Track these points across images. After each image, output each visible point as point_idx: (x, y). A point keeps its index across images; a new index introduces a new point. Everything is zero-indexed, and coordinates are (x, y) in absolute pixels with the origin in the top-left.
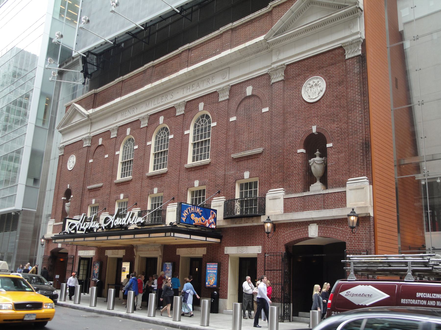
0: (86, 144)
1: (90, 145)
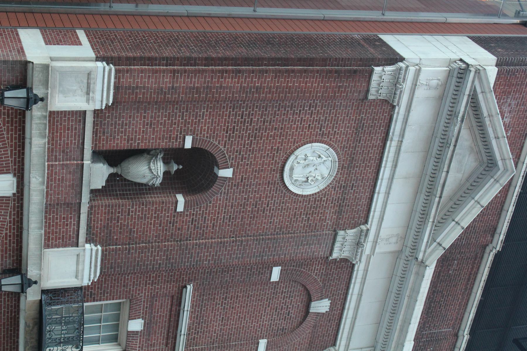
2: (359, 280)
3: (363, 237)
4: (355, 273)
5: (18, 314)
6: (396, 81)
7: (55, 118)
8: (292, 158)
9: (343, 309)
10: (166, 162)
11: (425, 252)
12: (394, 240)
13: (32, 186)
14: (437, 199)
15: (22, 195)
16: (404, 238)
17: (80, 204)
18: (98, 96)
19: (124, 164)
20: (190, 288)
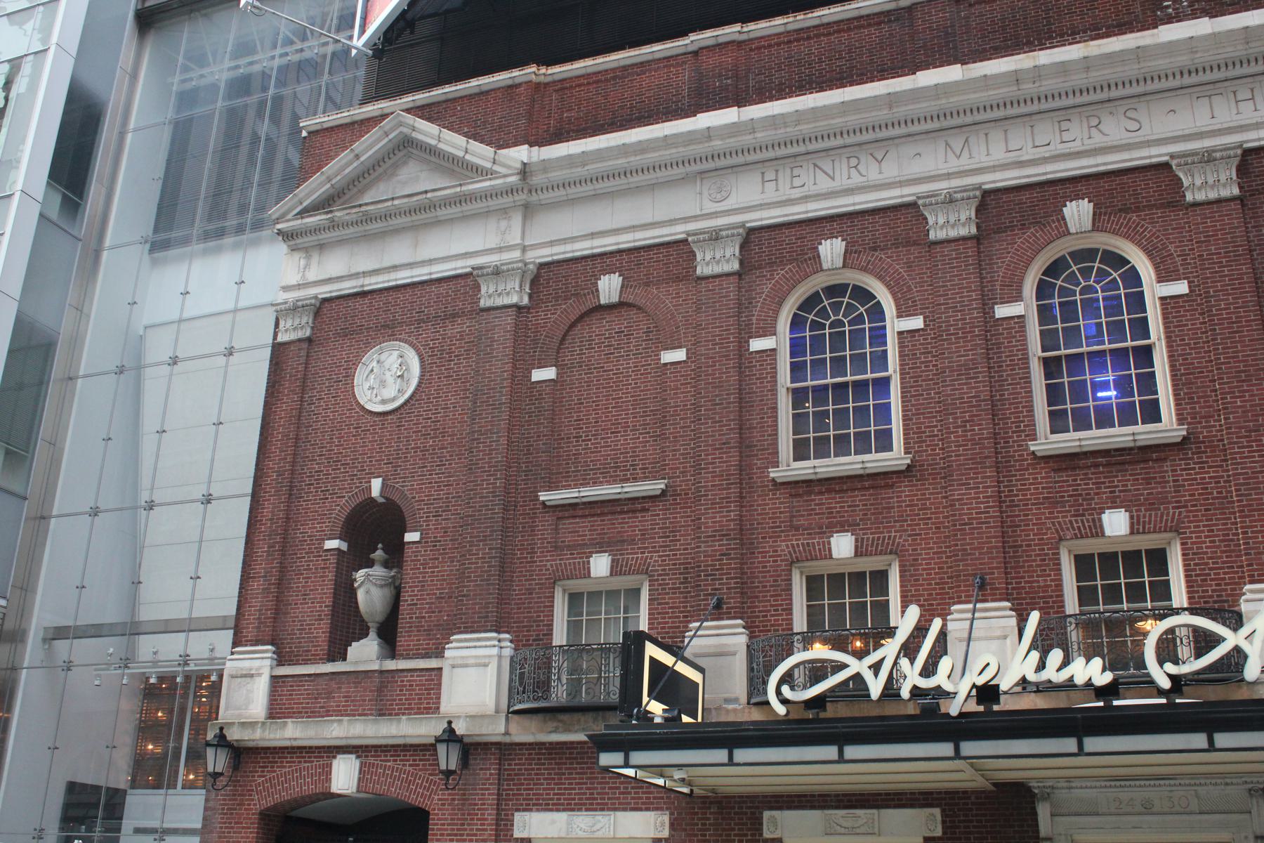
0: (513, 294)
1: (526, 301)
2: (569, 247)
3: (485, 271)
4: (555, 258)
5: (543, 744)
6: (295, 309)
7: (276, 711)
8: (369, 407)
9: (620, 252)
10: (370, 564)
11: (505, 176)
12: (503, 224)
13: (342, 734)
14: (429, 195)
15: (361, 747)
16: (504, 212)
17: (381, 672)
18: (257, 663)
19: (365, 616)
20: (544, 496)
